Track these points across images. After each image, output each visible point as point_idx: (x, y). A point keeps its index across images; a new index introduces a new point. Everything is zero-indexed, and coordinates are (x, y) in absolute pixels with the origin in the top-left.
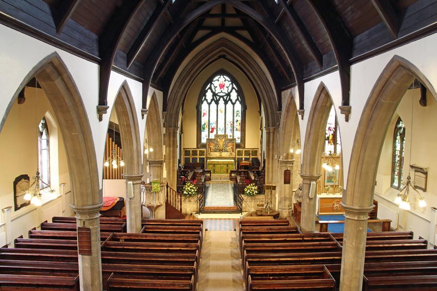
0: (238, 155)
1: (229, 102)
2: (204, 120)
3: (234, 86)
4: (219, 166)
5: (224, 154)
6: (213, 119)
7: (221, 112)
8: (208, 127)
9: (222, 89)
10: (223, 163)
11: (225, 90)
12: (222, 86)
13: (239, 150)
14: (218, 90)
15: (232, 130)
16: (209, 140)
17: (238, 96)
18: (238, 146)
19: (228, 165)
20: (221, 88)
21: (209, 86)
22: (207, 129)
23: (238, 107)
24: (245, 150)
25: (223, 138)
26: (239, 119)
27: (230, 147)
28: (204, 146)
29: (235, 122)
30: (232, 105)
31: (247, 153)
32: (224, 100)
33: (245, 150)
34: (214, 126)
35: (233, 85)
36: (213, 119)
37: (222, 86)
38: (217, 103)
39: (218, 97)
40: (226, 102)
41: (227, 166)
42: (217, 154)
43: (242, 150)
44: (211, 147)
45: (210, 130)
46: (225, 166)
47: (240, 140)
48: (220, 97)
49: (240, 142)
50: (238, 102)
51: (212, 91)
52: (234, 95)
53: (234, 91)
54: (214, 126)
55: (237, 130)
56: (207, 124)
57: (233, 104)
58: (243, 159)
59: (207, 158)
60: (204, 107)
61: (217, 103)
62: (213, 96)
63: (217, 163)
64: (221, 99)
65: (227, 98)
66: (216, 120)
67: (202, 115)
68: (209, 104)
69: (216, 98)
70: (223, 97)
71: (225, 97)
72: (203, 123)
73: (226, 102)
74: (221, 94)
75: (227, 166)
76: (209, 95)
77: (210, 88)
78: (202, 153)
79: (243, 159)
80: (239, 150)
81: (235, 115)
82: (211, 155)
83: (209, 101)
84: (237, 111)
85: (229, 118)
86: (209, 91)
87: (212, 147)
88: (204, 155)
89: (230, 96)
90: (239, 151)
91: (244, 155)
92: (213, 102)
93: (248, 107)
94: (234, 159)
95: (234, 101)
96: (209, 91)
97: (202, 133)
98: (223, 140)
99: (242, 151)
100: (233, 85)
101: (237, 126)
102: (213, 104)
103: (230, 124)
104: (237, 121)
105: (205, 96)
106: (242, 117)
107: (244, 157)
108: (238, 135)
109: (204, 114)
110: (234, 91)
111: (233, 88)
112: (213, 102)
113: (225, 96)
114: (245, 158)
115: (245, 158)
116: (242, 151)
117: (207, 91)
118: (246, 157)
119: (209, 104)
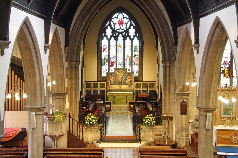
1: (128, 38)
2: (104, 54)
3: (132, 23)
4: (119, 98)
5: (123, 87)
6: (113, 54)
7: (120, 47)
9: (121, 26)
10: (123, 95)
11: (124, 27)
12: (121, 23)
13: (137, 82)
14: (117, 27)
15: (131, 65)
16: (109, 73)
17: (136, 32)
18: (136, 79)
19: (127, 96)
20: (119, 25)
21: (108, 23)
22: (107, 64)
23: (136, 42)
24: (143, 82)
25: (122, 72)
26: (137, 53)
27: (129, 80)
28: (104, 79)
29: (133, 57)
30: (130, 41)
31: (145, 85)
33: (143, 82)
34: (113, 60)
35: (131, 22)
36: (113, 54)
37: (121, 23)
38: (116, 39)
39: (117, 34)
40: (125, 39)
41: (127, 98)
42: (117, 87)
43: (140, 82)
45: (110, 64)
46: (125, 98)
48: (119, 33)
49: (138, 75)
50: (136, 38)
51: (111, 28)
52: (132, 32)
53: (132, 27)
54: (113, 60)
55: (135, 64)
56: (107, 59)
57: (132, 40)
58: (142, 91)
59: (107, 90)
60: (105, 42)
61: (116, 39)
64: (120, 35)
65: (125, 34)
66: (115, 55)
68: (109, 40)
69: (116, 34)
70: (121, 33)
71: (124, 34)
72: (103, 58)
73: (125, 39)
74: (120, 31)
75: (127, 98)
76: (109, 32)
77: (110, 25)
78: (102, 86)
79: (142, 91)
80: (137, 82)
81: (133, 50)
83: (109, 37)
84: (135, 47)
86: (109, 27)
87: (111, 80)
88: (105, 88)
89: (128, 32)
90: (137, 84)
91: (142, 87)
92: (113, 39)
94: (133, 91)
95: (132, 37)
96: (109, 27)
97: (103, 67)
98: (123, 73)
99: (141, 83)
100: (131, 22)
101: (135, 60)
102: (113, 40)
103: (128, 59)
104: (135, 56)
105: (105, 33)
106: (139, 52)
107: (142, 89)
108: (136, 68)
109: (104, 49)
110: (132, 27)
111: (131, 25)
112: (113, 39)
113: (123, 32)
114: (143, 91)
115: (143, 91)
116: (141, 83)
117: (106, 28)
118: (144, 89)
119: (109, 40)
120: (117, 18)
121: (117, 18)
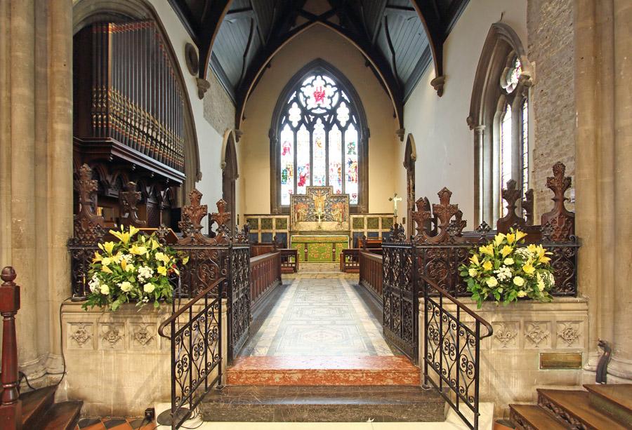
0: (355, 227)
1: (335, 126)
2: (286, 161)
3: (344, 95)
4: (316, 246)
5: (327, 226)
6: (303, 160)
8: (293, 174)
9: (320, 102)
11: (326, 104)
14: (312, 104)
16: (295, 197)
17: (350, 115)
18: (353, 210)
19: (334, 243)
20: (317, 100)
21: (294, 95)
23: (352, 135)
24: (369, 216)
26: (355, 158)
28: (286, 211)
29: (347, 166)
31: (373, 222)
32: (324, 122)
33: (369, 216)
35: (341, 94)
36: (303, 160)
37: (319, 96)
38: (310, 127)
39: (312, 118)
40: (328, 127)
42: (312, 226)
43: (362, 216)
44: (299, 211)
45: (298, 181)
46: (330, 247)
47: (357, 199)
48: (317, 116)
49: (356, 203)
50: (351, 127)
51: (300, 105)
52: (343, 113)
53: (343, 104)
54: (304, 171)
55: (351, 179)
56: (292, 169)
57: (343, 130)
60: (286, 135)
61: (310, 127)
62: (302, 115)
64: (319, 121)
65: (329, 118)
66: (308, 162)
67: (282, 151)
68: (296, 130)
69: (309, 119)
70: (321, 116)
71: (326, 117)
72: (283, 167)
73: (328, 127)
74: (319, 111)
76: (295, 114)
77: (297, 100)
78: (281, 224)
81: (347, 150)
82: (300, 227)
83: (295, 124)
84: (351, 144)
86: (295, 105)
89: (336, 115)
90: (355, 220)
91: (366, 226)
92: (303, 127)
94: (348, 232)
95: (343, 124)
96: (295, 105)
97: (282, 185)
99: (363, 219)
100: (341, 94)
101: (352, 171)
102: (303, 129)
103: (336, 169)
105: (288, 115)
108: (352, 189)
109: (285, 150)
110: (343, 104)
111: (341, 99)
112: (303, 127)
113: (325, 114)
114: (369, 233)
116: (363, 219)
118: (371, 230)
119: (296, 130)
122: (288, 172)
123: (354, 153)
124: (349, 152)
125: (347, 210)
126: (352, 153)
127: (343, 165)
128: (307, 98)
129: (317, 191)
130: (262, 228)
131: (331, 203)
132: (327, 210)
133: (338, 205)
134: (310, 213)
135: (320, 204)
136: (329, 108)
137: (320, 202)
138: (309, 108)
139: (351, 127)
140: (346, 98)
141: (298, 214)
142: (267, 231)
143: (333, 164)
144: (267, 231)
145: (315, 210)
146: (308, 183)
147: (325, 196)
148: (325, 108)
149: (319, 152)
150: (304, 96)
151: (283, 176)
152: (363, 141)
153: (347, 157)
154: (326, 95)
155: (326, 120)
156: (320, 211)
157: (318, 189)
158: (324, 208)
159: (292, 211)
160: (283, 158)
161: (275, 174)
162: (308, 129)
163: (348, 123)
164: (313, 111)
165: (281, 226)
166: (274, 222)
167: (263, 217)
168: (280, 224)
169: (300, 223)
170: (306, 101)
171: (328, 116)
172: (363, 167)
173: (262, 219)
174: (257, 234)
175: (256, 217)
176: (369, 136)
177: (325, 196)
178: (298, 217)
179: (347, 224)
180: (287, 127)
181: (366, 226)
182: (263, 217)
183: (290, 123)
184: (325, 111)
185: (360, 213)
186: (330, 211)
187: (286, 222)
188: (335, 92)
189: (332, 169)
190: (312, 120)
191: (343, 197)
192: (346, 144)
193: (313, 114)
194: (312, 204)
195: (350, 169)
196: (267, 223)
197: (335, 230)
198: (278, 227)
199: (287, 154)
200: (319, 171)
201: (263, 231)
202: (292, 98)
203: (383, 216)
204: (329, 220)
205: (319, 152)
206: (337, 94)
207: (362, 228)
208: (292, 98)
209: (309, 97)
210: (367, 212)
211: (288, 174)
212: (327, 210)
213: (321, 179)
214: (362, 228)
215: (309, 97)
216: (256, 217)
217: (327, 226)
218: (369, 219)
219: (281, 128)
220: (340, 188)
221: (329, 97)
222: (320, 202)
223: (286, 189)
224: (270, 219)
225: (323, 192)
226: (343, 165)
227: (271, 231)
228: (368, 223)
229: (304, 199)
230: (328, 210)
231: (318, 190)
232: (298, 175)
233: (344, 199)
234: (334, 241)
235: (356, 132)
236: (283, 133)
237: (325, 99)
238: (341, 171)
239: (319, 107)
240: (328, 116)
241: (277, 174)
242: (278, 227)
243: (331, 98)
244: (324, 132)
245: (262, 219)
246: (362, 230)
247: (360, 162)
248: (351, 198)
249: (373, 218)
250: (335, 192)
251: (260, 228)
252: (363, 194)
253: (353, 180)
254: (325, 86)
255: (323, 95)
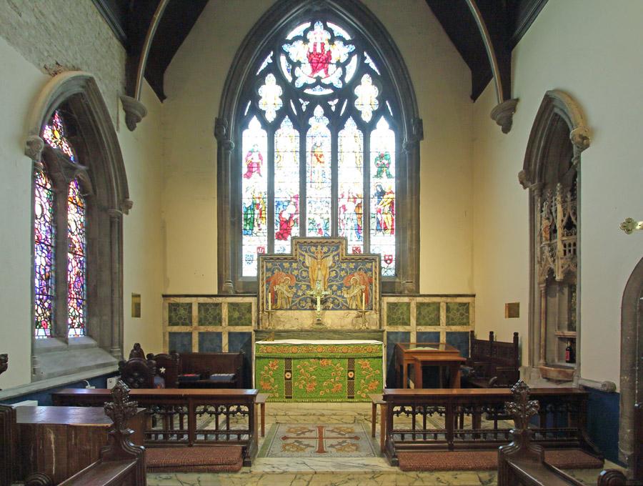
0: (390, 324)
1: (350, 123)
2: (252, 189)
3: (369, 60)
4: (311, 366)
5: (333, 319)
6: (287, 186)
7: (319, 158)
8: (265, 215)
9: (321, 73)
10: (332, 354)
11: (333, 76)
12: (320, 61)
13: (392, 300)
14: (304, 75)
15: (364, 229)
16: (267, 258)
17: (381, 99)
18: (388, 287)
19: (351, 360)
20: (315, 70)
21: (269, 60)
22: (264, 227)
23: (385, 138)
24: (419, 300)
25: (326, 255)
26: (390, 184)
27: (356, 291)
28: (250, 288)
29: (374, 202)
30: (360, 134)
31: (428, 312)
32: (328, 113)
33: (419, 300)
34: (290, 211)
35: (362, 59)
36: (287, 186)
37: (320, 61)
38: (302, 125)
39: (305, 104)
40: (336, 125)
41: (351, 368)
42: (304, 319)
43: (406, 300)
44: (276, 288)
45: (277, 228)
46: (342, 366)
47: (393, 265)
48: (314, 101)
49: (391, 273)
50: (383, 124)
51: (281, 80)
52: (367, 95)
53: (366, 79)
54: (290, 211)
55: (382, 227)
56: (264, 206)
57: (366, 128)
58: (413, 339)
59: (260, 334)
60: (253, 138)
61: (302, 125)
62: (285, 98)
63: (300, 353)
64: (319, 110)
65: (339, 106)
66: (297, 191)
67: (245, 170)
68: (271, 128)
69: (298, 106)
70: (323, 101)
71: (333, 104)
72: (246, 201)
73: (336, 125)
74: (318, 92)
75: (351, 368)
76: (270, 95)
77: (274, 68)
78: (240, 314)
79: (413, 339)
80: (392, 300)
81: (374, 170)
82: (279, 321)
83: (271, 117)
84: (381, 157)
85: (351, 181)
86: (271, 78)
87: (281, 288)
88: (249, 323)
89: (353, 98)
90: (392, 307)
91: (413, 321)
92: (287, 124)
93: (426, 128)
94: (377, 334)
95: (367, 117)
96: (271, 78)
97: (245, 239)
98: (329, 261)
99: (408, 304)
100: (362, 59)
101: (382, 211)
102: (287, 129)
103: (351, 207)
104: (382, 194)
105: (256, 98)
106: (400, 177)
107: (413, 328)
108: (385, 245)
109: (250, 167)
110: (366, 79)
111: (363, 69)
112: (287, 124)
113: (331, 97)
114: (419, 335)
115: (419, 335)
116: (408, 304)
117: (261, 80)
118: (423, 329)
119: (271, 128)
120: (306, 41)
121: (306, 41)
122: (257, 212)
123: (389, 175)
124: (379, 175)
125: (376, 287)
126: (384, 175)
127: (367, 198)
128: (294, 65)
129: (313, 249)
130: (201, 323)
131: (343, 273)
132: (335, 288)
133: (356, 277)
134: (300, 293)
135: (320, 275)
136: (340, 85)
137: (320, 270)
138: (299, 84)
139: (383, 124)
140: (373, 66)
141: (275, 294)
142: (211, 329)
143: (346, 196)
144: (211, 329)
145: (309, 287)
146: (295, 231)
147: (331, 258)
148: (331, 86)
149: (319, 171)
150: (289, 61)
151: (246, 220)
152: (408, 147)
153: (373, 181)
154: (334, 60)
155: (333, 109)
156: (319, 290)
157: (315, 243)
158: (329, 283)
159: (263, 288)
160: (245, 183)
161: (229, 213)
162: (296, 126)
163: (376, 115)
164: (308, 91)
165: (240, 318)
166: (225, 312)
167: (201, 300)
168: (236, 315)
169: (279, 313)
170: (293, 72)
171: (336, 101)
172: (408, 200)
173: (200, 305)
174: (190, 334)
175: (188, 300)
176: (420, 135)
177: (331, 258)
178: (274, 301)
179: (375, 316)
180: (254, 123)
181: (413, 321)
182: (201, 300)
183: (261, 115)
184: (330, 91)
185: (401, 294)
186: (340, 288)
187: (250, 311)
188: (351, 54)
189: (344, 207)
190: (304, 108)
191: (366, 260)
192: (373, 156)
193: (307, 97)
194: (304, 274)
195: (379, 207)
196: (210, 312)
197: (350, 327)
198: (232, 322)
199: (255, 175)
200: (318, 212)
201: (203, 329)
202: (264, 65)
203: (449, 300)
204: (337, 307)
205: (319, 171)
206: (355, 59)
207: (407, 323)
208: (264, 65)
209: (299, 64)
210: (415, 292)
211: (256, 216)
212: (335, 288)
213: (322, 226)
214: (407, 323)
215: (299, 64)
216: (188, 300)
217: (333, 319)
218: (420, 306)
219: (242, 124)
220: (360, 244)
221: (338, 64)
222: (320, 270)
223: (253, 244)
224: (217, 305)
225: (325, 249)
226: (367, 198)
227: (219, 329)
228: (419, 314)
229: (286, 265)
230: (337, 282)
231: (315, 245)
232: (276, 217)
233: (369, 265)
234: (351, 354)
235: (392, 134)
236: (246, 134)
237: (332, 68)
238: (361, 211)
239: (318, 82)
240: (336, 101)
241: (233, 215)
242: (232, 322)
243: (342, 65)
244: (328, 133)
245: (200, 305)
246: (408, 328)
247: (401, 191)
248: (384, 264)
249: (428, 304)
250: (350, 251)
251: (195, 323)
252: (408, 255)
253: (386, 229)
254: (331, 42)
255: (327, 60)
